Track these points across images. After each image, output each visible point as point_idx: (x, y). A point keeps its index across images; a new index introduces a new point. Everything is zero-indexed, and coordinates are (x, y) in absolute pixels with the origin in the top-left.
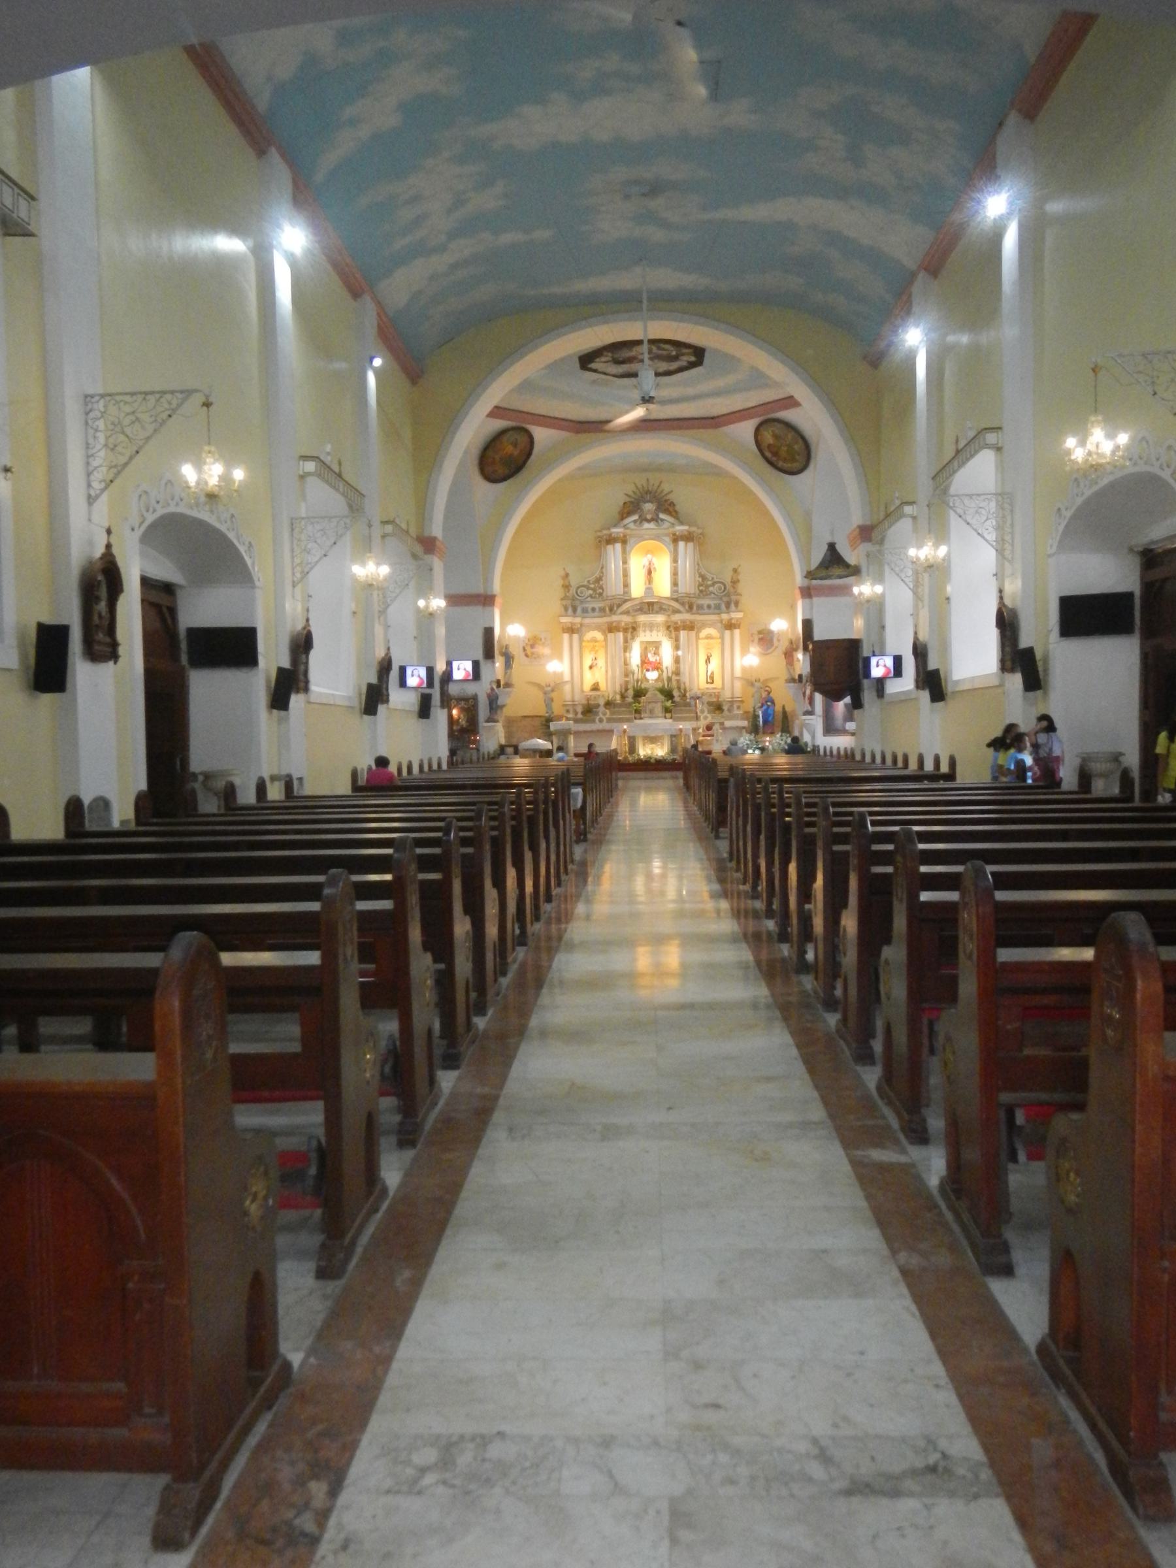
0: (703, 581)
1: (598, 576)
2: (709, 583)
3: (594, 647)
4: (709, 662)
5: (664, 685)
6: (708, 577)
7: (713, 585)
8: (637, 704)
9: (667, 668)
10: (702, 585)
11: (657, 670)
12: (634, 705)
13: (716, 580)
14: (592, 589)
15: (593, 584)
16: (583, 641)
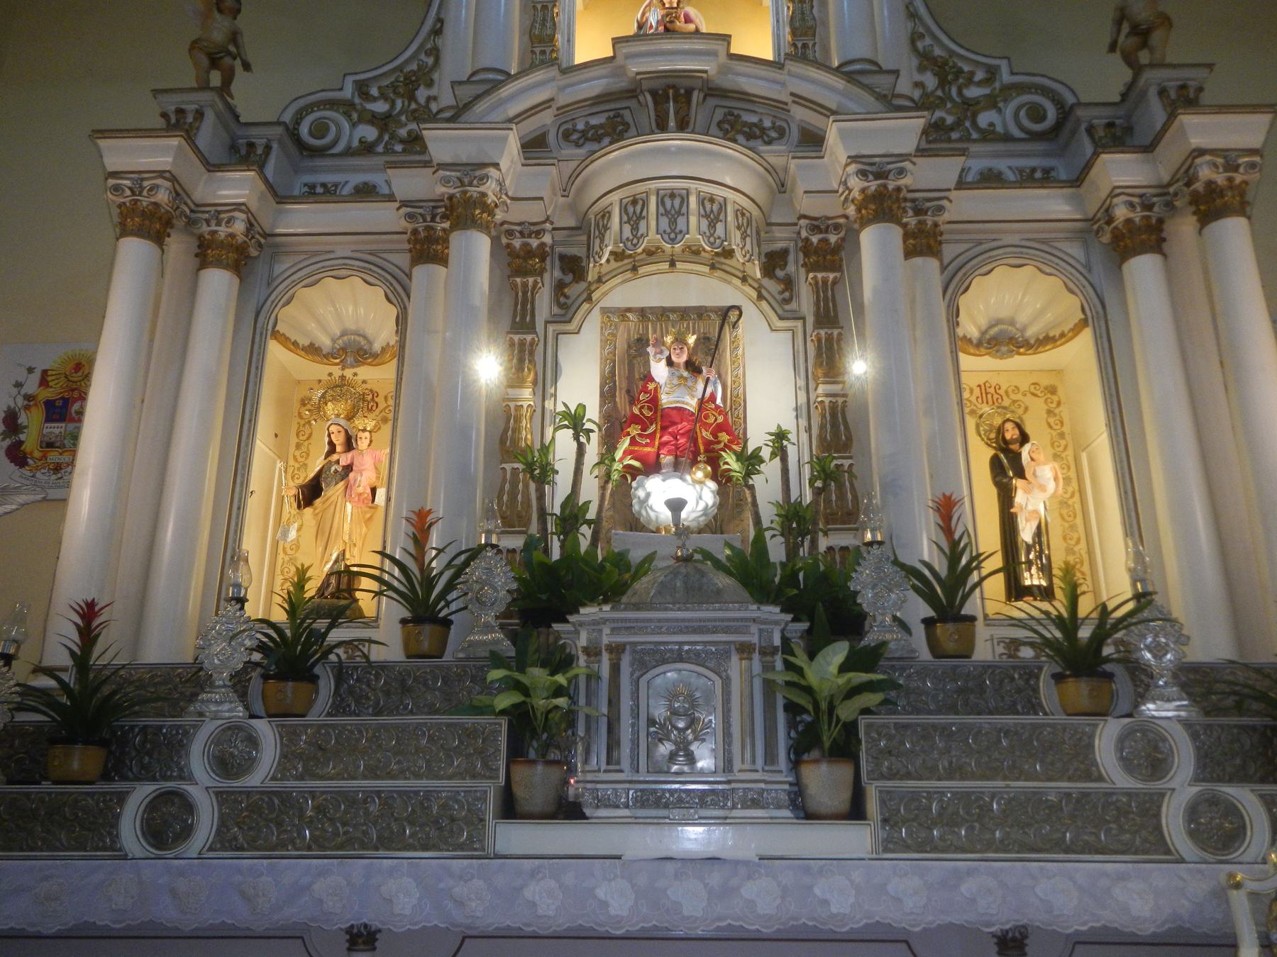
0: (943, 83)
1: (414, 67)
2: (973, 92)
3: (338, 388)
4: (1021, 473)
5: (759, 543)
6: (966, 68)
7: (992, 102)
8: (537, 675)
9: (780, 436)
10: (941, 103)
11: (714, 461)
12: (496, 674)
13: (1006, 78)
14: (374, 119)
15: (383, 96)
16: (276, 335)
